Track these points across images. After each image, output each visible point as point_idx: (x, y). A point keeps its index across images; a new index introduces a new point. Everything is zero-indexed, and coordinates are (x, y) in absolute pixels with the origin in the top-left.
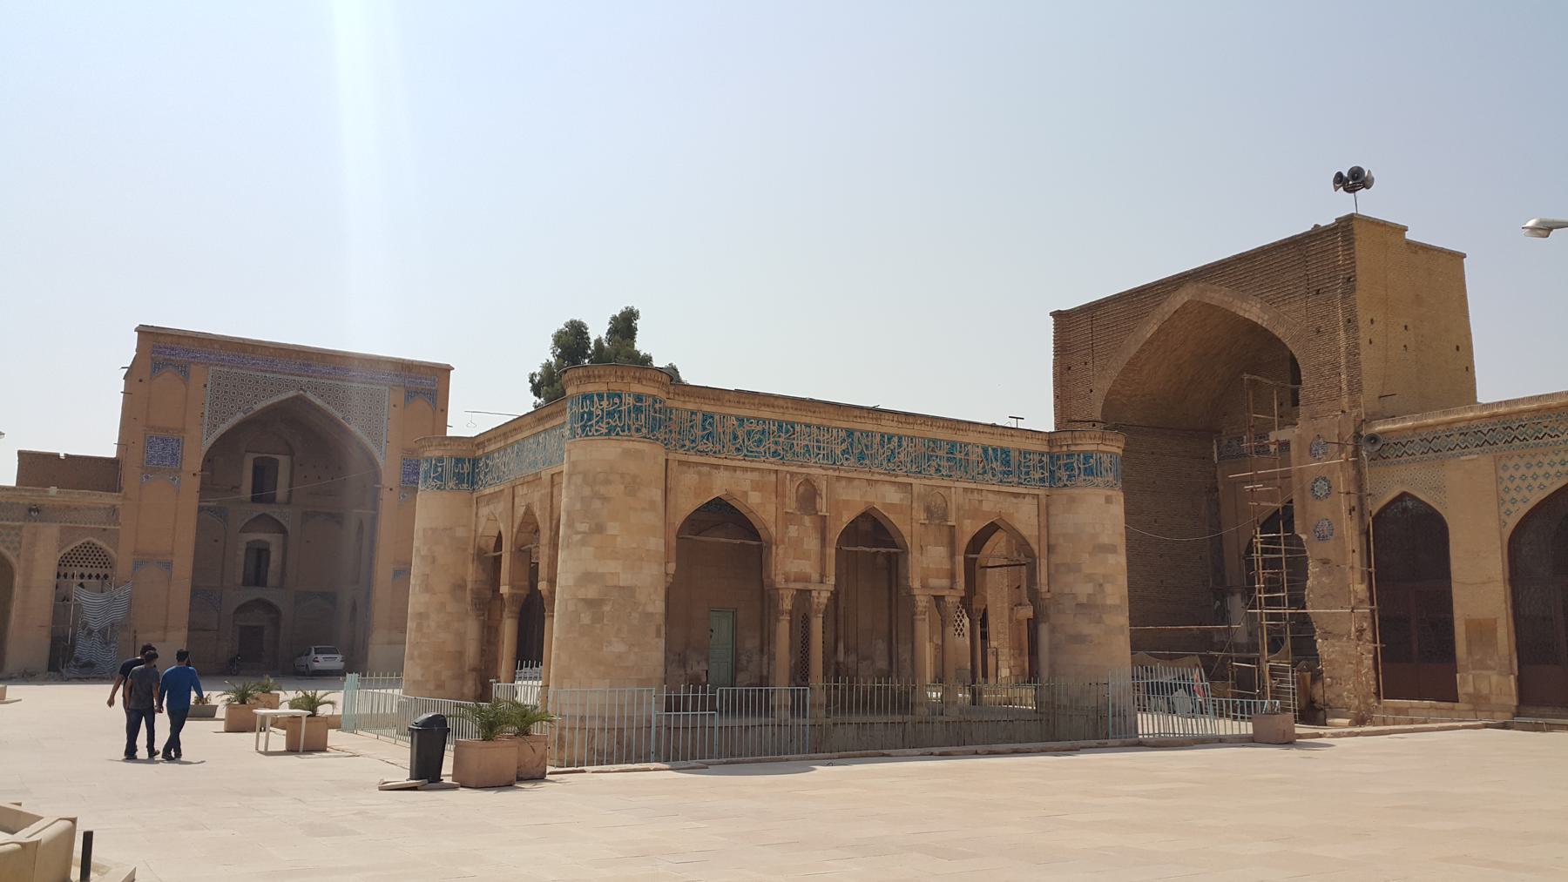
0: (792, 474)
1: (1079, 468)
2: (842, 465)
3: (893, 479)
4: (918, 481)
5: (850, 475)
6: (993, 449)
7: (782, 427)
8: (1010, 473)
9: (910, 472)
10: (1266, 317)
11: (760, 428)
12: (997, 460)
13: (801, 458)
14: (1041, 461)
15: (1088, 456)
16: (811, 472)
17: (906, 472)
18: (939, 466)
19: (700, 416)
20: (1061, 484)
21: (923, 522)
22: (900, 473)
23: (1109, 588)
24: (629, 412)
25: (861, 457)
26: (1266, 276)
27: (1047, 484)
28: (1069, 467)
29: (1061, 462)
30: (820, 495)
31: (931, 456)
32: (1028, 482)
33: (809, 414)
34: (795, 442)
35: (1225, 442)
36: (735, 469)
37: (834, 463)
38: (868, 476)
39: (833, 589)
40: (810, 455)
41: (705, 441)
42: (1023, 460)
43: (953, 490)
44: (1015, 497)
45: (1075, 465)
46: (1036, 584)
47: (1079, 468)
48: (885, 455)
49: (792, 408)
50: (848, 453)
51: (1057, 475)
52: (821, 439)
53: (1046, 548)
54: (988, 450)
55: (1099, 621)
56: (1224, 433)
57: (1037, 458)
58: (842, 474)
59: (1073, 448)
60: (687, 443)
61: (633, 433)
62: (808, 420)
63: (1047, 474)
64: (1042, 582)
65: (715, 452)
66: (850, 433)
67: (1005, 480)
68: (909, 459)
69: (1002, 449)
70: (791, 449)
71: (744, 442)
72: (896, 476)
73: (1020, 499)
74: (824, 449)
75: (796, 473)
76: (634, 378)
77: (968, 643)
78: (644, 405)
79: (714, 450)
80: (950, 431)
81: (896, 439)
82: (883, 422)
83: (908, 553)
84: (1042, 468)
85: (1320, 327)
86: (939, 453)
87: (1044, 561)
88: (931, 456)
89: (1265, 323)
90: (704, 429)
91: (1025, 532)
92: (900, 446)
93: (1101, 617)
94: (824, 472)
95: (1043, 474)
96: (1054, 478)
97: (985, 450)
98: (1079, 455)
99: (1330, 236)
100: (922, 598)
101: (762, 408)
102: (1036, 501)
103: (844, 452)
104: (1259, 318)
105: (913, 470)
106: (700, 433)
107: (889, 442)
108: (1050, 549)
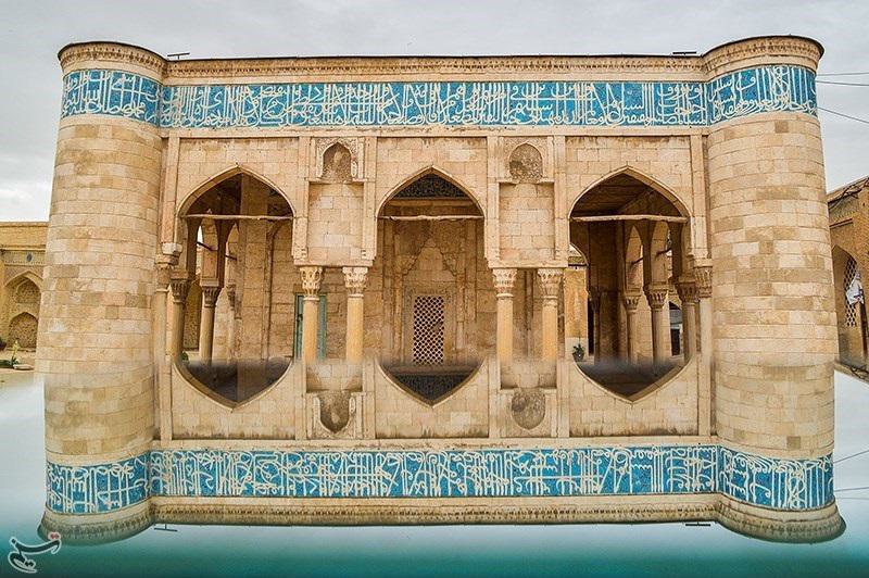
0: (318, 139)
1: (737, 93)
2: (386, 123)
3: (458, 134)
6: (613, 86)
8: (638, 113)
9: (484, 123)
12: (618, 99)
13: (330, 121)
14: (692, 94)
15: (748, 74)
18: (528, 113)
19: (208, 91)
22: (466, 125)
23: (781, 246)
24: (85, 89)
25: (413, 112)
29: (718, 89)
31: (516, 102)
33: (342, 72)
34: (323, 105)
36: (248, 140)
37: (376, 121)
39: (371, 264)
40: (343, 117)
41: (212, 115)
42: (662, 95)
47: (737, 93)
50: (396, 111)
52: (358, 98)
54: (604, 87)
55: (767, 292)
57: (686, 90)
60: (192, 119)
61: (87, 109)
62: (340, 79)
65: (224, 125)
66: (398, 86)
68: (483, 109)
70: (318, 112)
71: (258, 110)
73: (661, 144)
74: (361, 109)
76: (88, 54)
77: (860, 332)
78: (101, 80)
79: (222, 122)
81: (463, 88)
82: (443, 70)
86: (527, 98)
88: (516, 102)
90: (212, 102)
92: (468, 96)
93: (770, 286)
94: (360, 134)
95: (695, 109)
98: (736, 76)
101: (282, 73)
103: (387, 110)
105: (489, 121)
106: (206, 107)
107: (453, 92)
108: (709, 202)
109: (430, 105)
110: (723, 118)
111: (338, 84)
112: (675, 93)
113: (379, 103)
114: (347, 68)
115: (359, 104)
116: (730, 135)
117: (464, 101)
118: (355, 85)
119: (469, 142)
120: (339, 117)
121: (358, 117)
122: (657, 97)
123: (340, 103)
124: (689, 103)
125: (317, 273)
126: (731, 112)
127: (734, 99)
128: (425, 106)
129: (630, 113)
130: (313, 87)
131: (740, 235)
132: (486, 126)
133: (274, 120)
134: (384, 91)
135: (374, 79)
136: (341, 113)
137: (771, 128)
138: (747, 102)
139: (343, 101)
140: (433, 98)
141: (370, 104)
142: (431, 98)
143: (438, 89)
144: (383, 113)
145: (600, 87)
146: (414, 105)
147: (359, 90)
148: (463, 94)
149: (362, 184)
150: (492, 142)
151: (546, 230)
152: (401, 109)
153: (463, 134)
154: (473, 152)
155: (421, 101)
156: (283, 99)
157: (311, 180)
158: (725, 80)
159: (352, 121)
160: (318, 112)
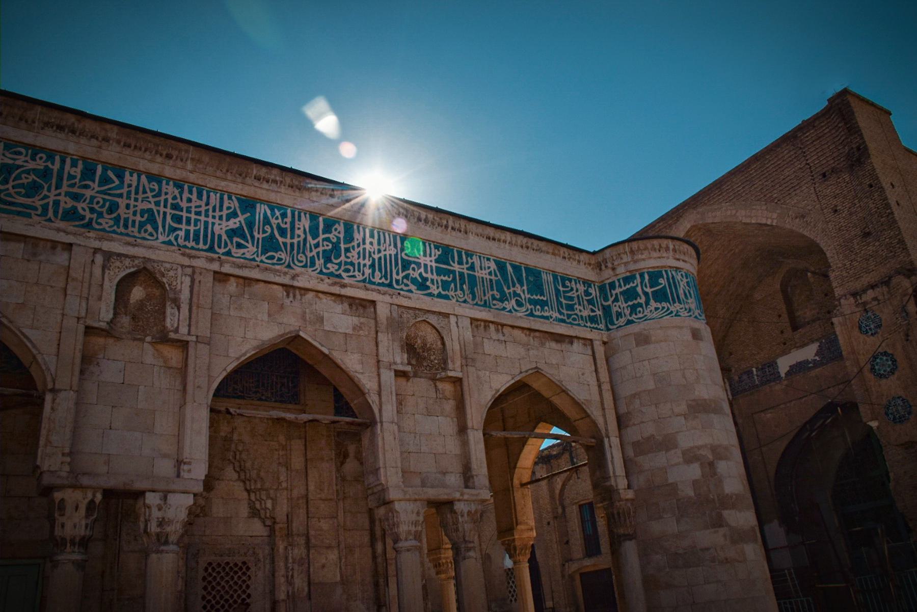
0: (109, 256)
1: (646, 294)
2: (228, 253)
3: (336, 290)
4: (387, 298)
5: (246, 273)
7: (94, 172)
10: (775, 216)
11: (39, 164)
14: (587, 293)
15: (655, 276)
16: (153, 257)
17: (364, 281)
20: (622, 321)
21: (400, 368)
22: (347, 281)
23: (722, 467)
25: (270, 245)
26: (773, 166)
27: (602, 326)
28: (630, 295)
29: (618, 290)
30: (177, 303)
32: (574, 319)
34: (122, 202)
35: (736, 378)
38: (286, 280)
42: (561, 289)
43: (453, 319)
44: (557, 341)
45: (639, 289)
46: (608, 478)
47: (646, 294)
48: (321, 249)
49: (118, 142)
50: (244, 237)
51: (615, 309)
52: (184, 205)
53: (615, 423)
56: (733, 371)
57: (582, 288)
58: (227, 269)
59: (632, 267)
62: (155, 168)
63: (599, 313)
64: (617, 474)
66: (248, 204)
67: (537, 313)
68: (368, 262)
69: (527, 269)
72: (344, 286)
75: (119, 255)
80: (439, 229)
81: (341, 228)
83: (376, 423)
84: (590, 302)
85: (836, 206)
87: (615, 441)
89: (775, 221)
91: (581, 395)
94: (186, 261)
96: (611, 316)
97: (501, 266)
98: (642, 275)
99: (823, 122)
100: (410, 506)
102: (589, 348)
103: (232, 233)
104: (767, 218)
109: (295, 241)
110: (629, 322)
111: (151, 177)
112: (572, 289)
113: (217, 221)
114: (169, 157)
115: (184, 214)
116: (643, 340)
117: (343, 246)
118: (179, 185)
119: (350, 305)
120: (149, 228)
121: (182, 234)
122: (558, 291)
123: (152, 206)
124: (585, 302)
125: (92, 502)
126: (641, 315)
127: (642, 300)
128: (288, 241)
129: (534, 303)
130: (105, 170)
131: (676, 456)
132: (373, 287)
133: (22, 205)
134: (226, 204)
135: (212, 183)
136: (152, 220)
137: (688, 336)
138: (659, 305)
139: (157, 204)
140: (300, 232)
141: (203, 218)
142: (297, 232)
143: (305, 223)
144: (224, 237)
145: (501, 266)
146: (272, 236)
147: (186, 195)
148: (342, 236)
149: (186, 343)
150: (383, 311)
151: (452, 446)
152: (252, 237)
153: (344, 292)
154: (356, 320)
155: (283, 232)
156: (46, 174)
157: (90, 322)
158: (627, 280)
159: (172, 238)
160: (110, 211)
